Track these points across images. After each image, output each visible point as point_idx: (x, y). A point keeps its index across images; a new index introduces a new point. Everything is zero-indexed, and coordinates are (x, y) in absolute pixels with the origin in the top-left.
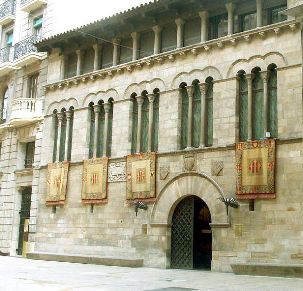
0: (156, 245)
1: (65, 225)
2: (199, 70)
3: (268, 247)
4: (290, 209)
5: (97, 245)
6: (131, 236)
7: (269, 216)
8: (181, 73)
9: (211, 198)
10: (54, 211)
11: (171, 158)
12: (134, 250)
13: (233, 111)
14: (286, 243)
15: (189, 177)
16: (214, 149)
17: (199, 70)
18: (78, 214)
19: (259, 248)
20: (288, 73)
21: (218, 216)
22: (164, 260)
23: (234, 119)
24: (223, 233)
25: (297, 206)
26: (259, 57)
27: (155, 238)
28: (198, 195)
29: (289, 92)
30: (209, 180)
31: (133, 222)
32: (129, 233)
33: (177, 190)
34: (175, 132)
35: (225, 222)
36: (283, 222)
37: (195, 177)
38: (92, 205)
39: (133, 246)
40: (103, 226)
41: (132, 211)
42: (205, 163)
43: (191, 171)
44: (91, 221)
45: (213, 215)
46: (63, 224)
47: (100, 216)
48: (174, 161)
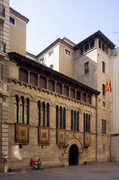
0: (66, 159)
1: (28, 154)
2: (76, 108)
3: (89, 157)
4: (92, 149)
5: (45, 161)
6: (58, 157)
7: (89, 151)
8: (72, 106)
9: (79, 145)
10: (20, 147)
11: (70, 132)
12: (59, 161)
13: (83, 123)
14: (91, 156)
15: (74, 139)
16: (80, 132)
17: (76, 108)
18: (36, 149)
19: (87, 158)
20: (92, 117)
21: (80, 150)
22: (68, 163)
23: (83, 125)
24: (81, 154)
25: (93, 148)
26: (88, 111)
27: (66, 157)
28: (76, 144)
29: (92, 122)
30: (79, 140)
31: (59, 152)
32: (58, 156)
33: (71, 143)
34: (70, 124)
35: (82, 152)
36: (91, 152)
37: (76, 139)
38: (42, 146)
39: (59, 160)
40: (47, 154)
41: (58, 148)
42: (78, 135)
43: (74, 137)
44: (42, 152)
45: (79, 150)
46: (27, 153)
47: (46, 150)
48: (70, 134)
